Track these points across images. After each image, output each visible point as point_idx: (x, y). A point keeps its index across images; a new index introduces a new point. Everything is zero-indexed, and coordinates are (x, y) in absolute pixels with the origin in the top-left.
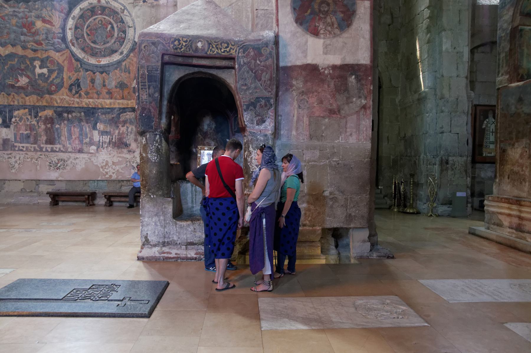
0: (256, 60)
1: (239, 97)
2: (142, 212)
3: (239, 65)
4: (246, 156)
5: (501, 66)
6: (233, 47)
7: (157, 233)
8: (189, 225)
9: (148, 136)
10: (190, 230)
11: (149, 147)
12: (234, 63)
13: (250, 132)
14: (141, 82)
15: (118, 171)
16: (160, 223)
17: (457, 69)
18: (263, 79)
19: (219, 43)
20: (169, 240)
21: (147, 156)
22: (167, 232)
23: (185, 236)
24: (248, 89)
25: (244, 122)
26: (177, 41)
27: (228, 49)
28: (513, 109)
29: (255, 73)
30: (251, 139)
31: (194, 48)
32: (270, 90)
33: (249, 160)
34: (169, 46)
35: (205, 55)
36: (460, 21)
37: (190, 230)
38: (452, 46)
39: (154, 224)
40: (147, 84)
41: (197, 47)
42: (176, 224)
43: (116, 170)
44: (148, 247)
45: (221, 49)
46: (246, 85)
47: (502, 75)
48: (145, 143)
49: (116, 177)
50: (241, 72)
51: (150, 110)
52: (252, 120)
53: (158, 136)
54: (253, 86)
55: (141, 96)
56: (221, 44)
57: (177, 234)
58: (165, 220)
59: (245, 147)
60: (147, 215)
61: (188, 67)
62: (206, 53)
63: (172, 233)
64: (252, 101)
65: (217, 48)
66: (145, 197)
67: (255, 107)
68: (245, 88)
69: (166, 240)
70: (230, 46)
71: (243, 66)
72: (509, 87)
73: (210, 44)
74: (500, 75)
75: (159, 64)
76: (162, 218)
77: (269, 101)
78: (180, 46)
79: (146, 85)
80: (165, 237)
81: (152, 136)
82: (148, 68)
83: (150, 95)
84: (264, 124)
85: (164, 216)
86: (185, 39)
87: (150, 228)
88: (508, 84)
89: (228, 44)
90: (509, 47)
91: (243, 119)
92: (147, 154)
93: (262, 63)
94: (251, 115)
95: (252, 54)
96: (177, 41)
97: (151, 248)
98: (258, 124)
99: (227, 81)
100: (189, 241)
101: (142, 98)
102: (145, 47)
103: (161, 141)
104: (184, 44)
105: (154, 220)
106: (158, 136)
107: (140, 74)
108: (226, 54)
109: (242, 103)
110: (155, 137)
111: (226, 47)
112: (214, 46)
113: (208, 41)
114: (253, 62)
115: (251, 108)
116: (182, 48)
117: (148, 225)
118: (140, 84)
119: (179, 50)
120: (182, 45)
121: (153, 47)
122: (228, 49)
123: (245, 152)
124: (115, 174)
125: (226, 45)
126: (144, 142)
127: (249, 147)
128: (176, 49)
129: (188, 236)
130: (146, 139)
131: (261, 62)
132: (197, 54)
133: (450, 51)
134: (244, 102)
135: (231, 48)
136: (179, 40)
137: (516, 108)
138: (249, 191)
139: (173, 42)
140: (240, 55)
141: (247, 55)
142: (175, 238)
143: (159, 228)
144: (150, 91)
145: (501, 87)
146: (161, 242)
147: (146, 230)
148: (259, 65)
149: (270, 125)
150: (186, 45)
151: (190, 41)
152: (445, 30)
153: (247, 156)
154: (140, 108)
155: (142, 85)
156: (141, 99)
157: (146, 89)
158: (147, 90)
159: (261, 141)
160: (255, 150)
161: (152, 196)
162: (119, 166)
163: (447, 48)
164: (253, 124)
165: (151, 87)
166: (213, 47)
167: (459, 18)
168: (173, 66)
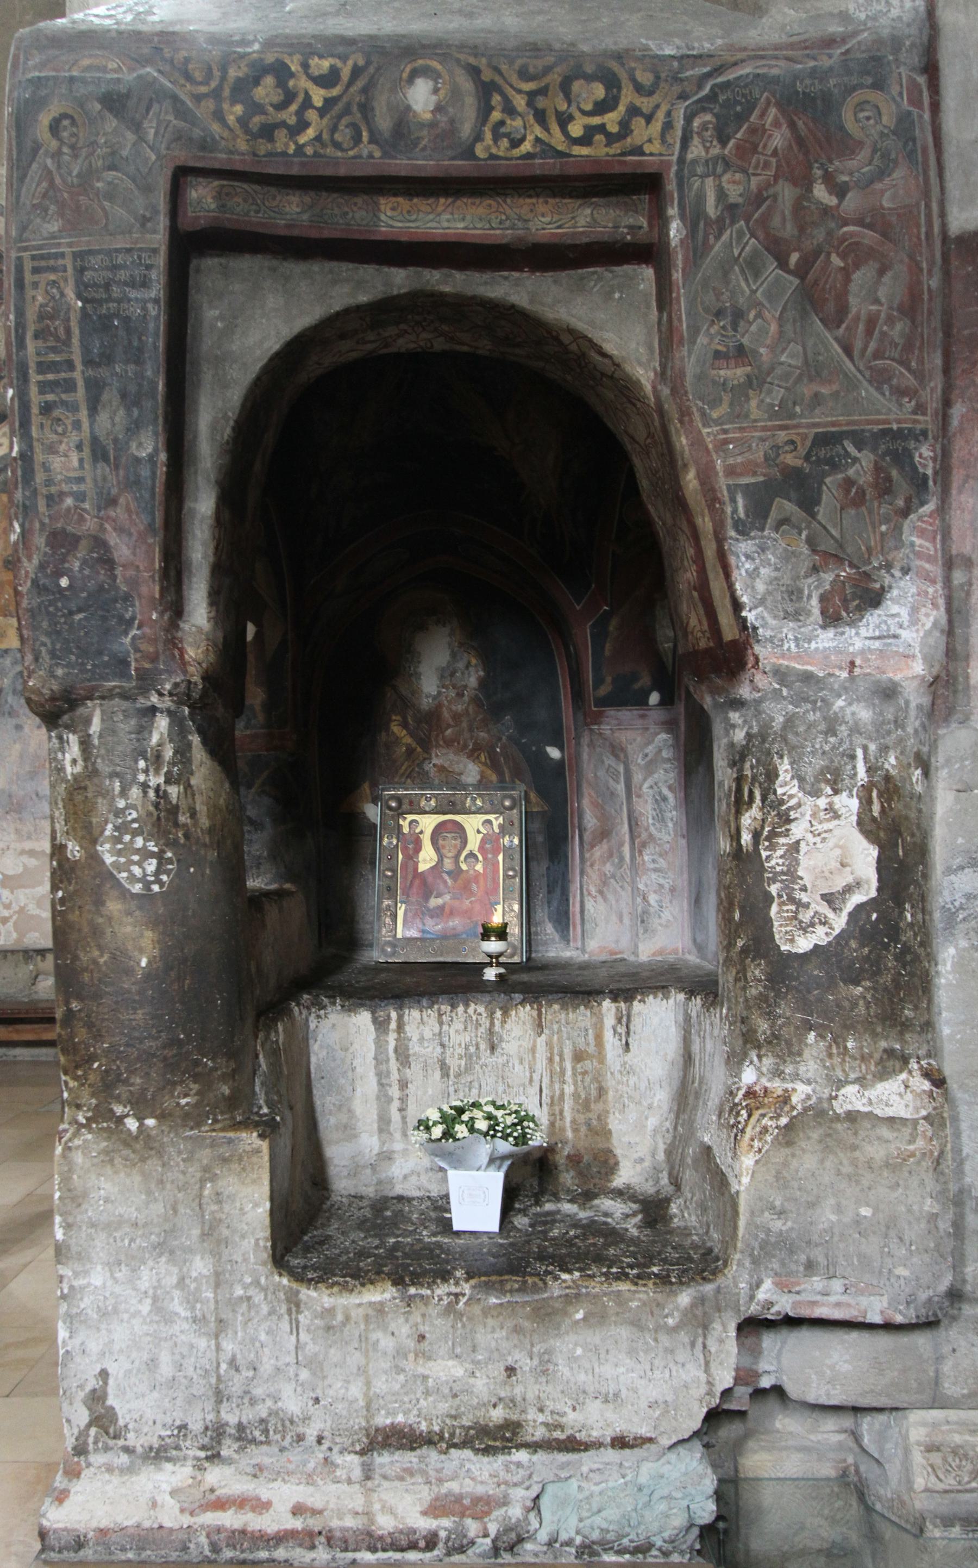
0: (806, 183)
1: (698, 442)
2: (68, 1227)
3: (694, 218)
4: (746, 838)
6: (645, 104)
7: (166, 1369)
8: (380, 1309)
9: (96, 726)
10: (386, 1343)
11: (106, 793)
12: (659, 218)
13: (781, 675)
14: (42, 367)
15: (22, 910)
16: (192, 1300)
18: (857, 304)
19: (554, 78)
20: (248, 1415)
21: (94, 858)
22: (233, 1364)
23: (356, 1391)
24: (754, 382)
25: (737, 606)
26: (269, 80)
27: (611, 120)
29: (802, 271)
30: (790, 721)
31: (384, 123)
32: (910, 381)
33: (775, 860)
34: (219, 116)
35: (461, 167)
37: (386, 1343)
39: (146, 1307)
40: (77, 375)
41: (403, 116)
42: (294, 1304)
43: (15, 907)
44: (110, 1469)
45: (564, 121)
46: (741, 354)
48: (78, 769)
49: (15, 935)
50: (708, 264)
51: (99, 543)
52: (794, 594)
53: (162, 723)
54: (790, 357)
55: (39, 457)
56: (565, 87)
57: (304, 1374)
58: (218, 1280)
59: (739, 780)
60: (100, 1246)
61: (345, 269)
62: (469, 153)
63: (267, 1366)
64: (790, 459)
65: (541, 117)
66: (87, 1126)
67: (809, 504)
68: (736, 374)
69: (231, 1417)
70: (628, 96)
71: (720, 226)
73: (486, 90)
75: (159, 237)
76: (200, 1266)
77: (903, 459)
78: (289, 115)
79: (70, 386)
80: (219, 1396)
81: (126, 727)
82: (81, 271)
83: (98, 452)
84: (873, 618)
85: (216, 1254)
86: (322, 65)
87: (120, 1333)
89: (612, 83)
91: (731, 587)
92: (94, 842)
93: (852, 202)
94: (788, 556)
95: (778, 139)
96: (269, 80)
97: (129, 1470)
98: (831, 619)
99: (609, 348)
100: (383, 1420)
101: (47, 469)
102: (55, 128)
103: (183, 752)
104: (318, 96)
105: (146, 1279)
106: (162, 723)
107: (31, 314)
108: (599, 150)
109: (722, 483)
110: (143, 730)
111: (602, 107)
112: (520, 102)
113: (474, 72)
114: (786, 193)
115: (785, 506)
116: (303, 125)
117: (104, 1314)
118: (34, 377)
119: (282, 141)
120: (307, 103)
121: (111, 123)
122: (611, 120)
123: (738, 813)
124: (10, 924)
125: (599, 91)
126: (74, 762)
127: (772, 775)
128: (268, 132)
129: (381, 1385)
130: (85, 744)
131: (840, 191)
132: (402, 165)
134: (731, 471)
135: (634, 111)
136: (281, 72)
138: (777, 1073)
139: (242, 89)
140: (696, 150)
141: (748, 149)
142: (292, 1404)
143: (183, 1330)
144: (103, 418)
146: (196, 1426)
147: (94, 1347)
148: (826, 211)
149: (914, 622)
150: (329, 103)
151: (356, 72)
153: (756, 835)
154: (40, 541)
155: (44, 387)
156: (40, 477)
157: (74, 408)
158: (83, 414)
159: (856, 729)
160: (816, 793)
161: (132, 1124)
162: (27, 891)
164: (796, 615)
165: (110, 395)
166: (510, 110)
168: (245, 263)
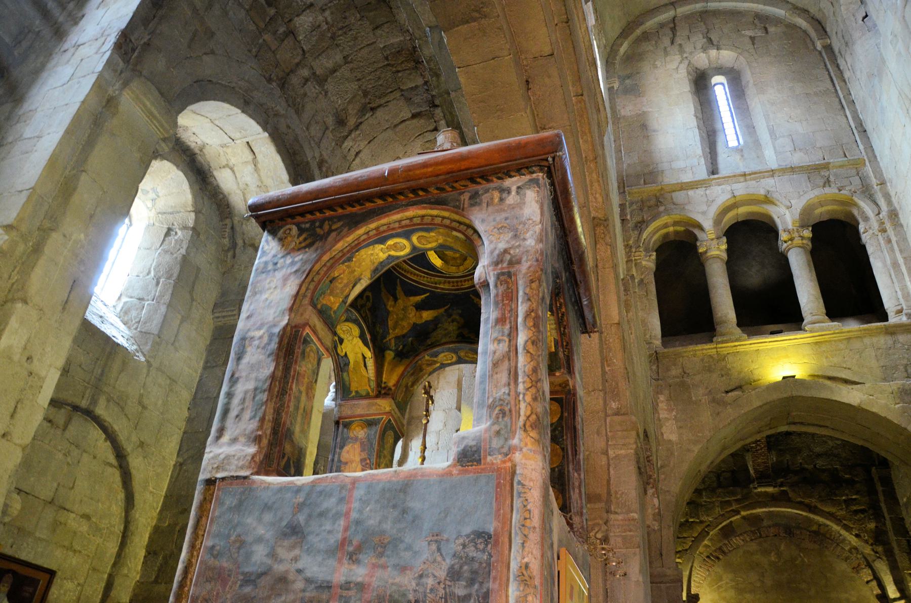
5: (233, 413)
17: (12, 416)
28: (260, 554)
36: (66, 302)
38: (25, 348)
47: (234, 440)
72: (254, 482)
74: (226, 438)
88: (252, 474)
90: (272, 369)
133: (16, 358)
137: (273, 555)
145: (223, 479)
152: (25, 302)
163: (10, 347)
167: (66, 295)
